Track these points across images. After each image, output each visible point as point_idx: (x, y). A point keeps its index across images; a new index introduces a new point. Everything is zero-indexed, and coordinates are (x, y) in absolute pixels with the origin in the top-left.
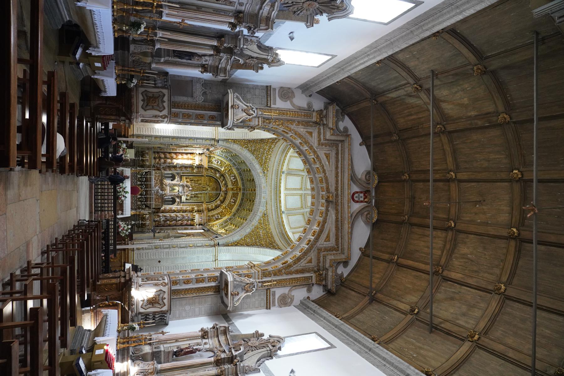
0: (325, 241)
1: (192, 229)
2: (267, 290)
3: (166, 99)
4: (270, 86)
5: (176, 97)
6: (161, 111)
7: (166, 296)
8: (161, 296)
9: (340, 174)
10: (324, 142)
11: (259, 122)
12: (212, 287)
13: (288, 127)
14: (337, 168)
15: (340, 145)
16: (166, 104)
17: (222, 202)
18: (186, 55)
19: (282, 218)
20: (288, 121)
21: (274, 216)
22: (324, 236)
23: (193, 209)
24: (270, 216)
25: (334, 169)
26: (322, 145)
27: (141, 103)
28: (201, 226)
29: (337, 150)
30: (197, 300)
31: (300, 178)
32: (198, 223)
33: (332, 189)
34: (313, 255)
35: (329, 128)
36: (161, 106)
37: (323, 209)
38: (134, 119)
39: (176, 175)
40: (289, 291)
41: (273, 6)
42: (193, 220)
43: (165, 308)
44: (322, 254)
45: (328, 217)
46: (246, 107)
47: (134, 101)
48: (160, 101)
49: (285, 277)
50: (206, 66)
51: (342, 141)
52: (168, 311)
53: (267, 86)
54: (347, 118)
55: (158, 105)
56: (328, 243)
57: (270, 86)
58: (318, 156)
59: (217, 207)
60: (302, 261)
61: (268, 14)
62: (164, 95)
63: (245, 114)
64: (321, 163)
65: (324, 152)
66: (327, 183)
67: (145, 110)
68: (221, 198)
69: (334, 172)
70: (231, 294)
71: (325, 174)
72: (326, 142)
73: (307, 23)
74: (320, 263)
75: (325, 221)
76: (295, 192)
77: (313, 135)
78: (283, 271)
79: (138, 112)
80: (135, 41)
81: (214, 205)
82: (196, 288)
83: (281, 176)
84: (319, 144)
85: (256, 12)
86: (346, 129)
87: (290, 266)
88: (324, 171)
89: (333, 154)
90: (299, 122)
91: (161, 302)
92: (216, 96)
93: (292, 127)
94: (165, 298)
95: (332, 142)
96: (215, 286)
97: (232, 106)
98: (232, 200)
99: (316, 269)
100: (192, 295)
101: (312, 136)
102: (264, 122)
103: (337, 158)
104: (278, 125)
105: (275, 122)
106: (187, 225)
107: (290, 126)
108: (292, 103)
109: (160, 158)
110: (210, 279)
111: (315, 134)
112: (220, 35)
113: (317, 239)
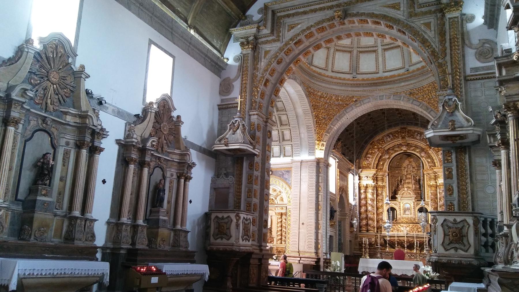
0: (399, 9)
2: (466, 80)
3: (220, 215)
4: (218, 105)
5: (229, 205)
6: (232, 221)
7: (451, 218)
8: (450, 225)
9: (313, 8)
10: (275, 34)
11: (254, 115)
12: (456, 157)
13: (260, 81)
14: (305, 13)
15: (279, 14)
16: (225, 215)
18: (159, 194)
19: (414, 71)
20: (253, 81)
21: (412, 82)
22: (392, 13)
24: (411, 87)
25: (305, 17)
26: (279, 36)
27: (224, 241)
29: (284, 16)
30: (479, 177)
31: (361, 55)
33: (329, 13)
34: (418, 23)
35: (259, 32)
36: (226, 220)
37: (355, 19)
38: (239, 249)
39: (388, 207)
40: (471, 48)
41: (66, 113)
43: (470, 220)
44: (418, 10)
45: (366, 12)
46: (231, 130)
47: (221, 248)
48: (223, 221)
49: (448, 58)
50: (179, 175)
51: (274, 13)
52: (475, 217)
53: (219, 109)
54: (249, 13)
55: (226, 223)
56: (402, 5)
57: (218, 105)
58: (291, 40)
60: (426, 37)
61: (76, 116)
62: (217, 217)
63: (238, 131)
64: (298, 35)
65: (286, 32)
66: (323, 21)
67: (231, 237)
69: (310, 16)
70: (453, 129)
71: (312, 26)
72: (275, 32)
73: (81, 77)
74: (431, 11)
75: (372, 15)
76: (380, 59)
77: (268, 49)
78: (440, 61)
79: (233, 244)
80: (133, 244)
82: (458, 179)
83: (358, 80)
84: (279, 40)
85: (74, 128)
86: (260, 11)
87: (433, 53)
88: (308, 28)
89: (289, 21)
90: (254, 69)
91: (460, 226)
92: (230, 163)
93: (260, 75)
94: (455, 220)
95: (275, 25)
96: (456, 153)
97: (226, 145)
98: (418, 138)
99: (439, 15)
100: (469, 185)
101: (269, 51)
102: (255, 109)
103: (293, 15)
104: (258, 92)
105: (255, 95)
107: (258, 79)
108: (236, 79)
109: (367, 225)
110: (448, 160)
111: (267, 47)
112: (123, 161)
113: (396, 21)
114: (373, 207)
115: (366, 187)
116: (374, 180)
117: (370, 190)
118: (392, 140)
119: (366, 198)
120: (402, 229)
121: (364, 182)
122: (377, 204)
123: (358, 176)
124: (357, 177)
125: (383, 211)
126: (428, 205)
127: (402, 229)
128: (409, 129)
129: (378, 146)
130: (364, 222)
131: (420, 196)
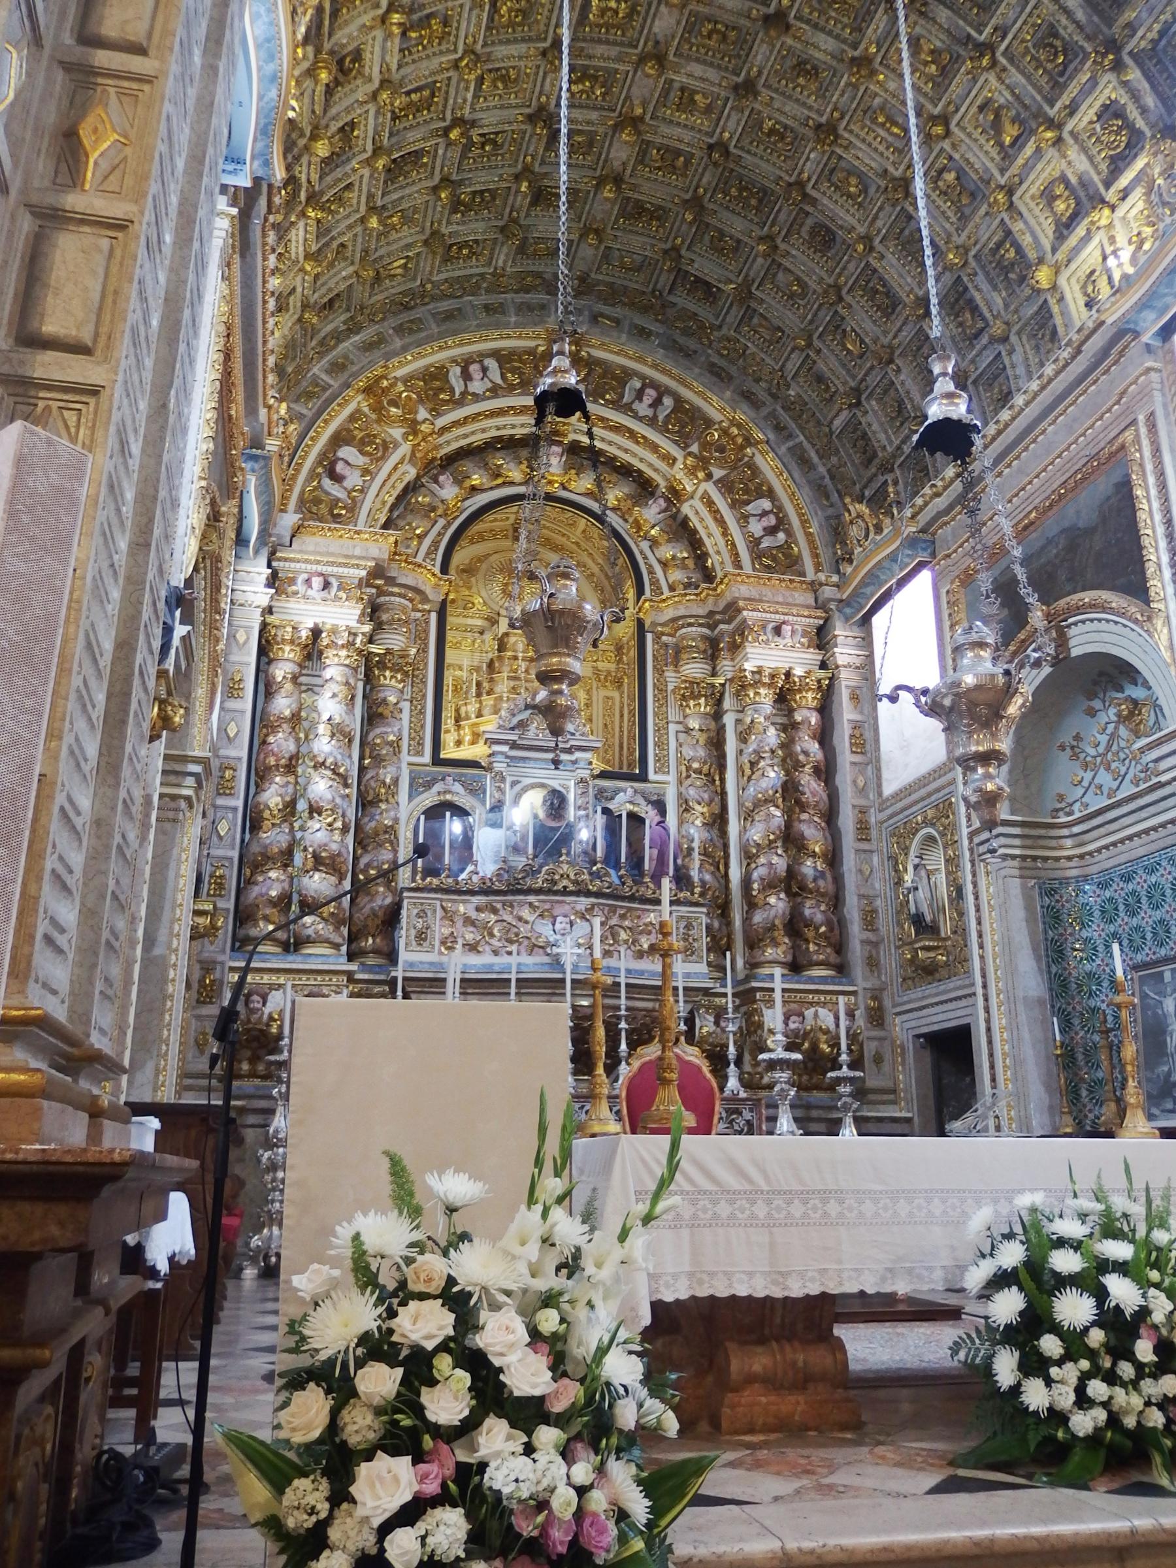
17: (644, 488)
23: (691, 691)
28: (842, 632)
39: (429, 799)
59: (682, 531)
81: (667, 551)
115: (313, 649)
117: (336, 668)
118: (495, 391)
120: (544, 929)
122: (362, 769)
125: (396, 820)
127: (544, 929)
128: (598, 354)
130: (273, 882)
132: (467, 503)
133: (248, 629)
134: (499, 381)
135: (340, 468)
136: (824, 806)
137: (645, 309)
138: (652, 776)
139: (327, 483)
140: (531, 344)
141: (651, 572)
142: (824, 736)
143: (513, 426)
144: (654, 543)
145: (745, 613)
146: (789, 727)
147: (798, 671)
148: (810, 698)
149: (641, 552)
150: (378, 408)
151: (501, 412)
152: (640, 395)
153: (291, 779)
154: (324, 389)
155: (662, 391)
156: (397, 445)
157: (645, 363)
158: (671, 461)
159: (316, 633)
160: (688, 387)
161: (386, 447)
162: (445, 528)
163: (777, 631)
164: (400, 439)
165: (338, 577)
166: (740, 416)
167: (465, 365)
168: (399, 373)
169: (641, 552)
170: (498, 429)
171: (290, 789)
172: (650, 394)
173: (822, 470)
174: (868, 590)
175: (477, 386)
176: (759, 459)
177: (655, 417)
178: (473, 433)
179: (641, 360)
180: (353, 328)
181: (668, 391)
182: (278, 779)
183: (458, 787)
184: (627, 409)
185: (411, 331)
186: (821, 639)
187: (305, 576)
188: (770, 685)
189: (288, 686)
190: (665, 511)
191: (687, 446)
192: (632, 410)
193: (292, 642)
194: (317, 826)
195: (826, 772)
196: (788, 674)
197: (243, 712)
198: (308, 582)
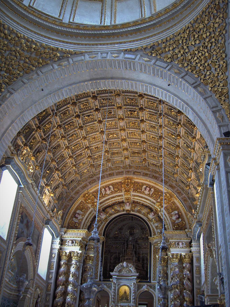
1: (199, 259)
17: (151, 210)
32: (187, 249)
42: (181, 259)
68: (145, 211)
106: (191, 271)
114: (74, 286)
116: (81, 247)
118: (112, 193)
119: (67, 273)
121: (68, 249)
123: (59, 239)
124: (58, 241)
126: (154, 288)
128: (136, 180)
129: (93, 200)
131: (144, 276)
132: (110, 217)
133: (55, 254)
134: (113, 190)
135: (77, 215)
136: (190, 289)
137: (145, 169)
138: (152, 281)
139: (74, 219)
140: (120, 180)
141: (153, 230)
142: (191, 271)
143: (119, 199)
144: (154, 223)
145: (170, 240)
146: (182, 269)
147: (183, 254)
148: (187, 260)
149: (151, 225)
150: (85, 200)
151: (114, 197)
152: (145, 189)
153: (64, 287)
154: (74, 198)
155: (150, 187)
156: (90, 208)
157: (148, 181)
158: (155, 204)
159: (70, 253)
160: (157, 185)
161: (88, 208)
162: (105, 224)
163: (178, 244)
164: (90, 207)
165: (75, 240)
166: (169, 191)
167: (105, 188)
168: (91, 192)
169: (151, 225)
170: (115, 200)
171: (63, 289)
172: (148, 189)
173: (190, 202)
174: (195, 233)
175: (108, 192)
176: (175, 201)
177: (149, 194)
178: (109, 202)
179: (146, 180)
180: (79, 184)
181: (153, 187)
182: (60, 287)
183: (105, 286)
184: (144, 193)
185: (93, 183)
186: (190, 245)
187: (68, 240)
188: (176, 258)
189: (64, 266)
190: (154, 215)
191: (157, 200)
192: (144, 193)
193: (65, 256)
194: (68, 297)
195: (191, 280)
196: (181, 255)
197: (53, 273)
198: (69, 242)
